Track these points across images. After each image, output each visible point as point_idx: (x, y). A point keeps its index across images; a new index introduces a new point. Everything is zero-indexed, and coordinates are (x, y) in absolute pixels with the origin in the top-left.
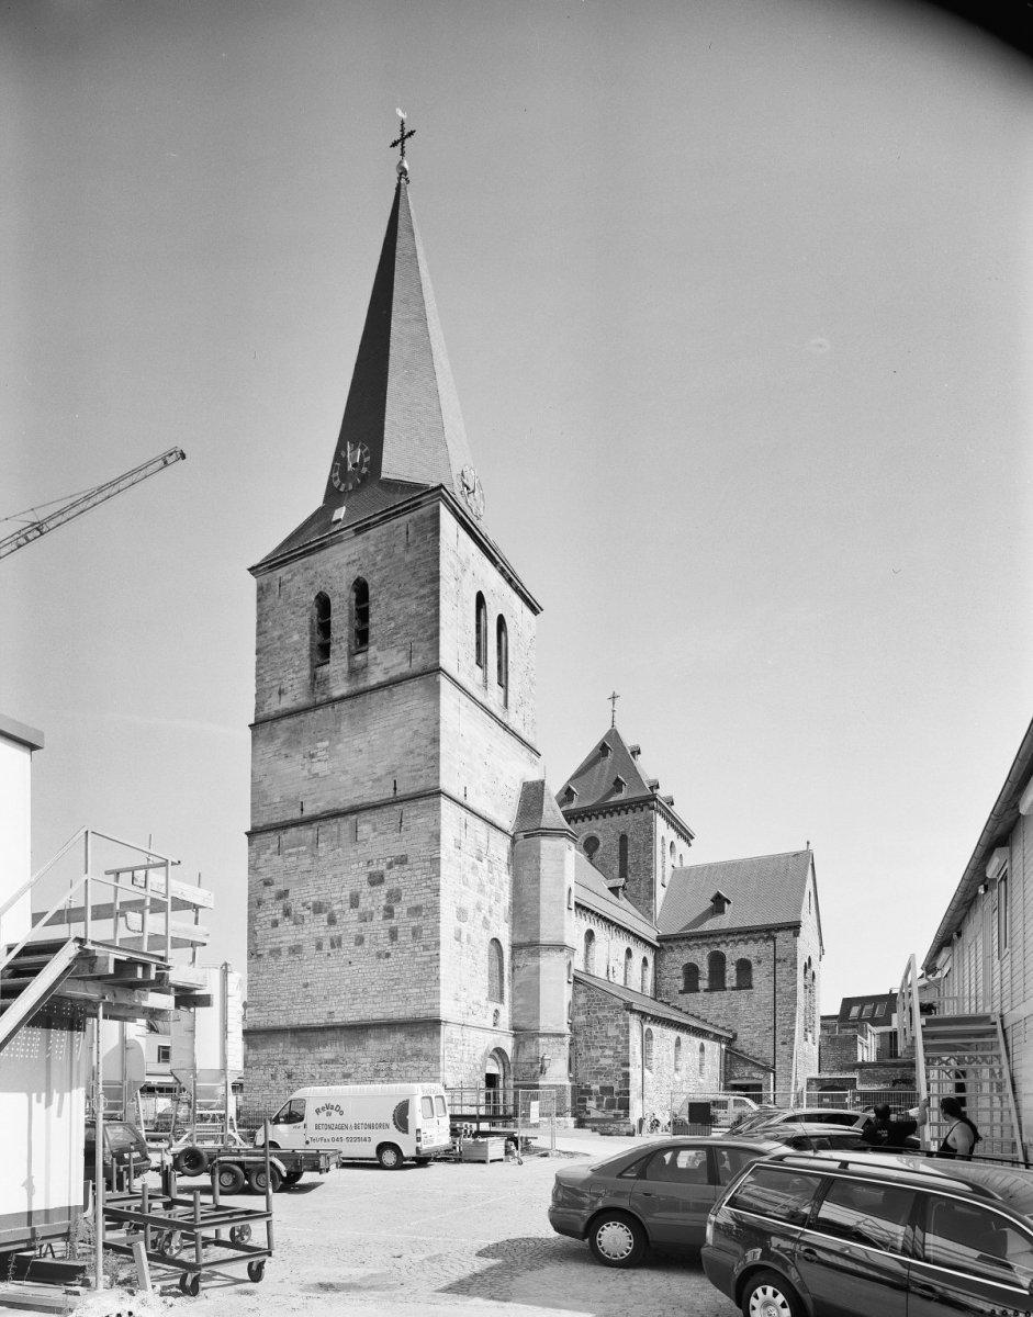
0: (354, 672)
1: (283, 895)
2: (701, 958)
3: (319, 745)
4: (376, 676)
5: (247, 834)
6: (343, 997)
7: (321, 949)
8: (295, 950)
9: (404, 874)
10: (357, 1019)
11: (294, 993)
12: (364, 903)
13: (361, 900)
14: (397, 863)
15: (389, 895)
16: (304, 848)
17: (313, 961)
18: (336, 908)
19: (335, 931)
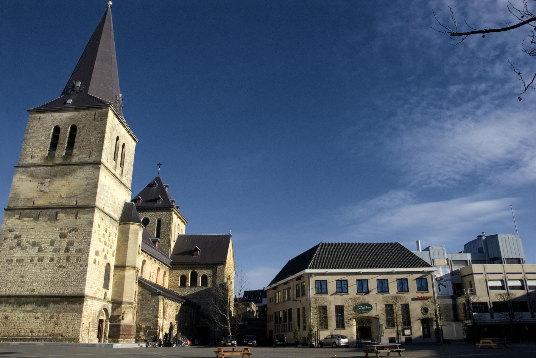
3: (46, 180)
4: (75, 160)
13: (55, 244)
15: (68, 244)
18: (43, 245)
19: (41, 255)
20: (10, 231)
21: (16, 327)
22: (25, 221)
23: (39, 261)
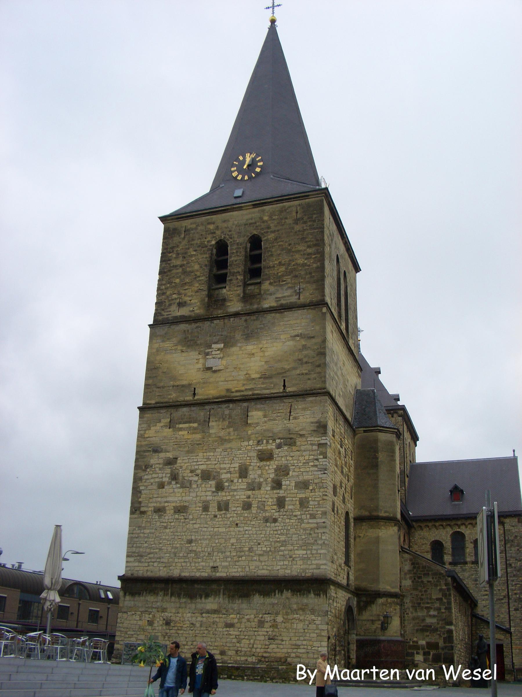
0: (246, 298)
1: (171, 462)
3: (214, 346)
5: (139, 408)
6: (228, 554)
7: (208, 511)
8: (181, 510)
9: (292, 454)
10: (242, 574)
11: (176, 548)
12: (252, 475)
14: (285, 445)
16: (195, 425)
17: (198, 521)
18: (224, 476)
19: (223, 496)
20: (156, 451)
21: (190, 643)
22: (181, 429)
23: (220, 509)
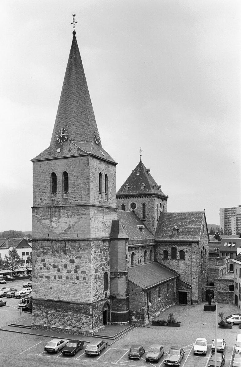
2: (169, 249)
12: (69, 268)
18: (60, 267)
